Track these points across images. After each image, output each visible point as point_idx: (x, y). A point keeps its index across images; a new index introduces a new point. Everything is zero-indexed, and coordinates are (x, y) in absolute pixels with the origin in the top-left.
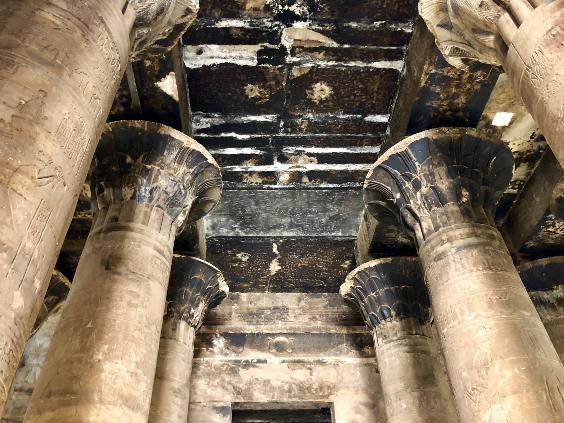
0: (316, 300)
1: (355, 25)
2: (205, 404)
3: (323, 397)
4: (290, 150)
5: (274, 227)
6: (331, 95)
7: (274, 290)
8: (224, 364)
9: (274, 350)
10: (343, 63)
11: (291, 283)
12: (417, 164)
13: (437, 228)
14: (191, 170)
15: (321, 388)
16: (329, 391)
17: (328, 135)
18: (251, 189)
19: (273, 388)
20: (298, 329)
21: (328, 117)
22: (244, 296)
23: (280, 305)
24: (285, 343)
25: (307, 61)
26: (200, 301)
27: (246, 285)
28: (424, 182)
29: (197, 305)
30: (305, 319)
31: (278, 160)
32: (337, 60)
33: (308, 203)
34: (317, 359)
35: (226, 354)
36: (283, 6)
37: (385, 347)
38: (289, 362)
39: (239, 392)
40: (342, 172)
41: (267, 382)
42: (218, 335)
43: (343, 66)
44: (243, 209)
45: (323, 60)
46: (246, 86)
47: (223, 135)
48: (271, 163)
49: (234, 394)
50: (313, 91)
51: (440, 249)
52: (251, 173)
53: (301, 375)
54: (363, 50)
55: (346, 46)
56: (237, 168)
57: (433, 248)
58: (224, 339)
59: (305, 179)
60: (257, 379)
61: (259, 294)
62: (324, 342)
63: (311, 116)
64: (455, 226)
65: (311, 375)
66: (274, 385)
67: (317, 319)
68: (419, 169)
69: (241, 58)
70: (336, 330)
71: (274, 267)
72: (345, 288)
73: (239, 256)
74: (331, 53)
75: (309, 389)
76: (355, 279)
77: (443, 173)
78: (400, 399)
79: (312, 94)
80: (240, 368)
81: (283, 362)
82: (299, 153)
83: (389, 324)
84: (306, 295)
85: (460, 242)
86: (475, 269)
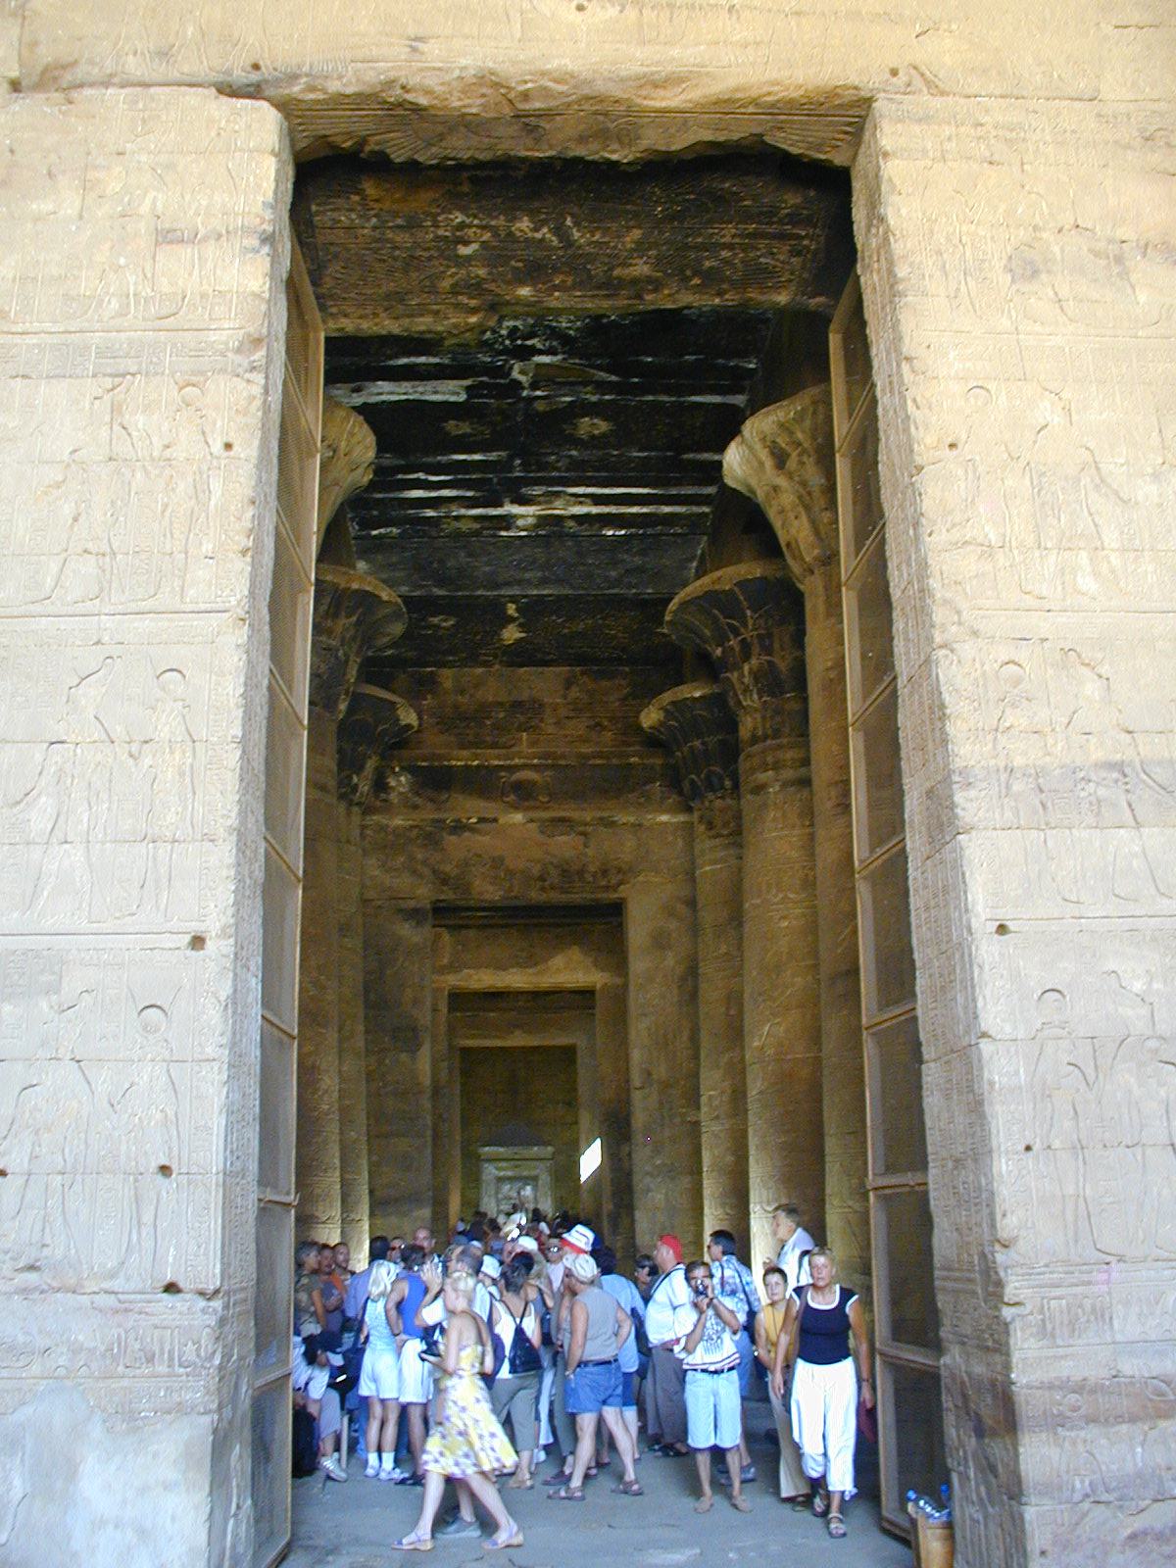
0: (605, 683)
2: (379, 903)
3: (607, 888)
4: (537, 491)
5: (508, 584)
7: (511, 664)
8: (412, 827)
9: (512, 797)
11: (549, 653)
12: (749, 613)
13: (765, 737)
14: (354, 619)
15: (605, 872)
16: (620, 876)
18: (458, 535)
19: (511, 873)
20: (563, 756)
22: (447, 677)
23: (525, 696)
24: (534, 783)
26: (365, 757)
27: (451, 658)
28: (756, 649)
29: (362, 767)
30: (578, 727)
31: (512, 502)
32: (618, 394)
33: (578, 553)
34: (599, 814)
35: (415, 807)
36: (513, 340)
37: (708, 844)
38: (542, 821)
39: (444, 880)
41: (497, 862)
42: (397, 769)
44: (441, 561)
45: (594, 394)
46: (446, 422)
47: (400, 476)
48: (501, 505)
49: (434, 883)
51: (763, 777)
52: (457, 518)
53: (565, 845)
56: (430, 513)
57: (753, 770)
58: (409, 777)
59: (571, 523)
60: (480, 856)
61: (480, 670)
62: (614, 783)
64: (788, 743)
65: (586, 846)
66: (511, 867)
67: (604, 728)
68: (750, 622)
69: (436, 393)
70: (641, 757)
71: (511, 634)
72: (650, 717)
73: (435, 620)
75: (581, 873)
76: (666, 711)
77: (786, 639)
78: (719, 937)
80: (444, 834)
81: (532, 821)
82: (557, 494)
83: (718, 803)
84: (583, 673)
85: (788, 774)
86: (798, 823)
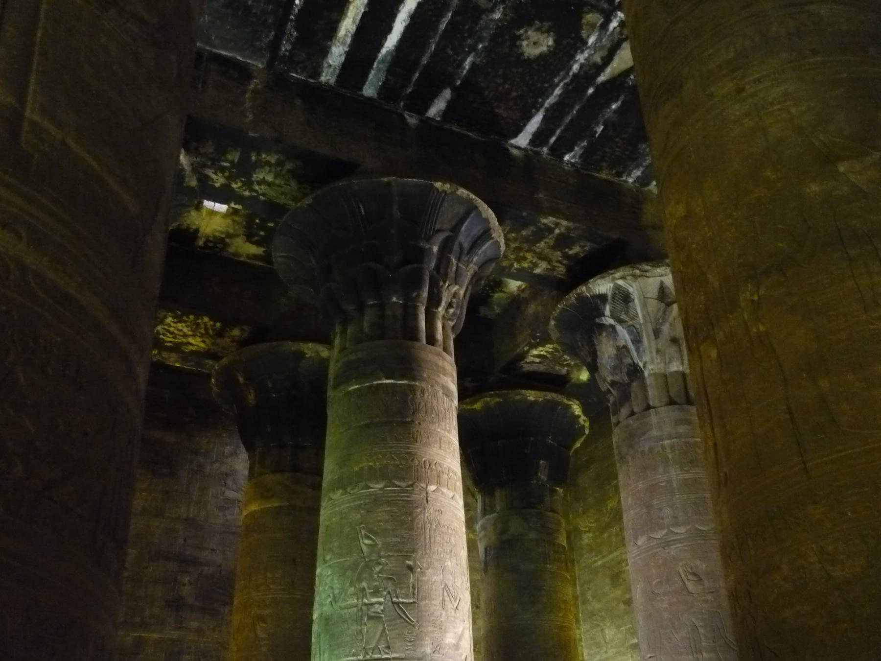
1: (614, 107)
6: (522, 54)
10: (566, 81)
17: (440, 32)
21: (480, 39)
25: (599, 39)
32: (575, 76)
40: (332, 30)
43: (561, 81)
45: (587, 59)
50: (543, 33)
54: (572, 107)
55: (591, 91)
63: (497, 16)
74: (593, 71)
79: (538, 30)
